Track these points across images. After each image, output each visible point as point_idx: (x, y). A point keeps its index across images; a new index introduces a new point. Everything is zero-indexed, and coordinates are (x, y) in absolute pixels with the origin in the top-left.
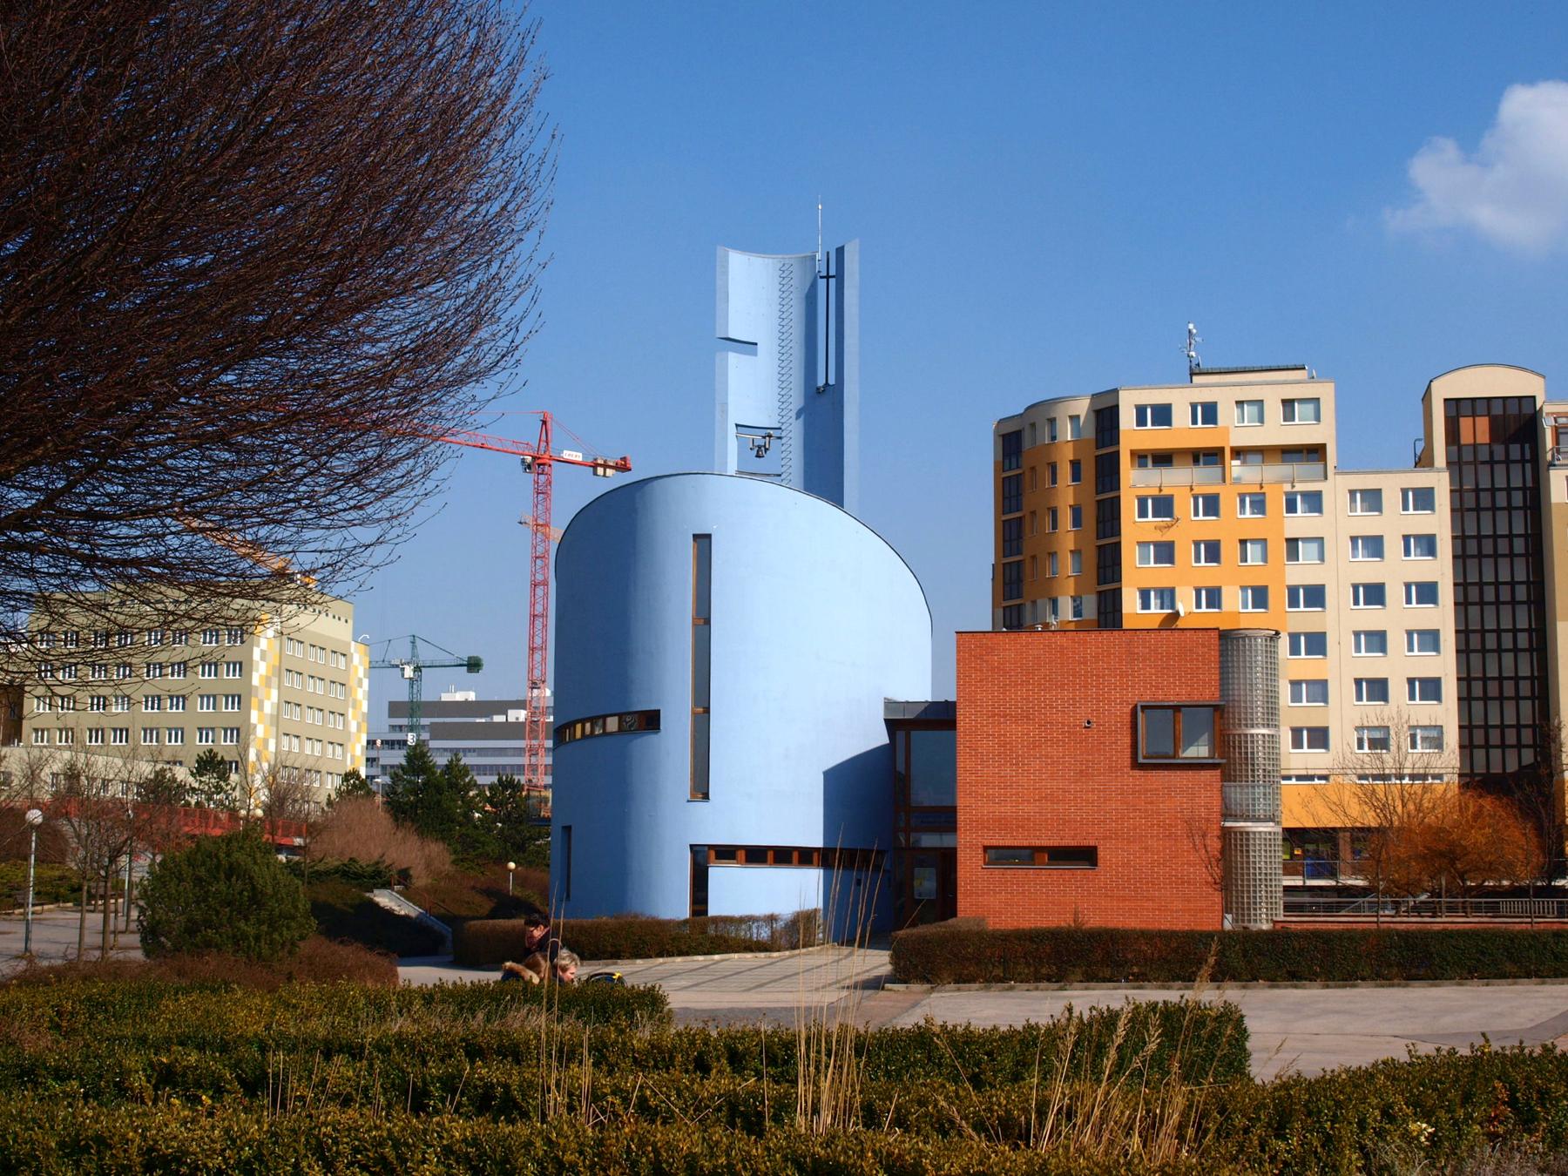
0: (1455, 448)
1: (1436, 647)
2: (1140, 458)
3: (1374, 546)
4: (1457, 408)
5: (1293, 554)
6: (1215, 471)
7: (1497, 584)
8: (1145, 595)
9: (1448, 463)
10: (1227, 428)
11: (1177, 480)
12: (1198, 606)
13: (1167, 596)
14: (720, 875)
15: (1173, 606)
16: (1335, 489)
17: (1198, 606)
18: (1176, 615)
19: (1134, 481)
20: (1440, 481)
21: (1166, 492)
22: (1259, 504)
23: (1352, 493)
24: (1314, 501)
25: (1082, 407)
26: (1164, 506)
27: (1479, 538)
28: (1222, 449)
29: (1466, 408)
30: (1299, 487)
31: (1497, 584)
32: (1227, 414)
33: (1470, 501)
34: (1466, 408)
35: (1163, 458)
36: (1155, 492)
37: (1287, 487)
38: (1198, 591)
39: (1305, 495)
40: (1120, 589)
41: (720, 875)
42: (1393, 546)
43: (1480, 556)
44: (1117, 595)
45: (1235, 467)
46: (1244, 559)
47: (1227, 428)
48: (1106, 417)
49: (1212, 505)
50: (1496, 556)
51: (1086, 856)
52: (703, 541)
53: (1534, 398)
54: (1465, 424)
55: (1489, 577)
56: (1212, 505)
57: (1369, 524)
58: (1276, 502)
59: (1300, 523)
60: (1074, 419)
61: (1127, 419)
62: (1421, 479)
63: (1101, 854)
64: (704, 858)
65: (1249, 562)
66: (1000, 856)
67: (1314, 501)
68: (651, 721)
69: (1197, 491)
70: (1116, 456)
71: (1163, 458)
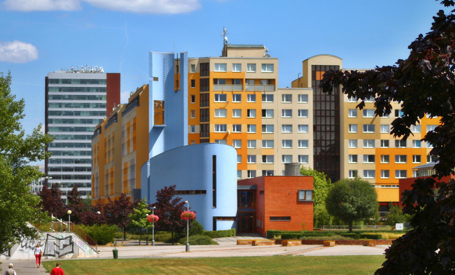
0: (314, 81)
1: (307, 145)
2: (215, 81)
3: (289, 112)
4: (315, 68)
5: (264, 115)
6: (239, 87)
7: (326, 125)
8: (217, 126)
9: (313, 86)
10: (244, 73)
11: (227, 89)
12: (234, 130)
13: (224, 127)
14: (219, 223)
15: (225, 130)
16: (278, 95)
17: (234, 130)
18: (227, 134)
19: (214, 89)
20: (310, 93)
21: (224, 93)
22: (253, 97)
23: (283, 95)
24: (271, 98)
25: (196, 63)
26: (223, 97)
27: (321, 110)
28: (242, 80)
29: (318, 68)
30: (266, 93)
31: (326, 125)
32: (244, 68)
33: (318, 99)
34: (318, 68)
35: (223, 81)
36: (221, 93)
37: (263, 93)
38: (234, 126)
39: (268, 95)
40: (209, 124)
41: (219, 223)
42: (295, 113)
43: (321, 116)
44: (208, 126)
45: (246, 86)
46: (249, 115)
47: (244, 73)
48: (205, 67)
49: (239, 98)
50: (326, 116)
51: (289, 218)
52: (214, 157)
53: (339, 66)
54: (318, 73)
55: (323, 123)
56: (239, 98)
57: (287, 106)
58: (259, 96)
59: (266, 105)
60: (193, 66)
61: (212, 69)
62: (303, 92)
63: (292, 218)
64: (215, 219)
65: (250, 117)
66: (272, 218)
67: (271, 98)
68: (204, 192)
69: (234, 93)
70: (208, 79)
71: (223, 81)
